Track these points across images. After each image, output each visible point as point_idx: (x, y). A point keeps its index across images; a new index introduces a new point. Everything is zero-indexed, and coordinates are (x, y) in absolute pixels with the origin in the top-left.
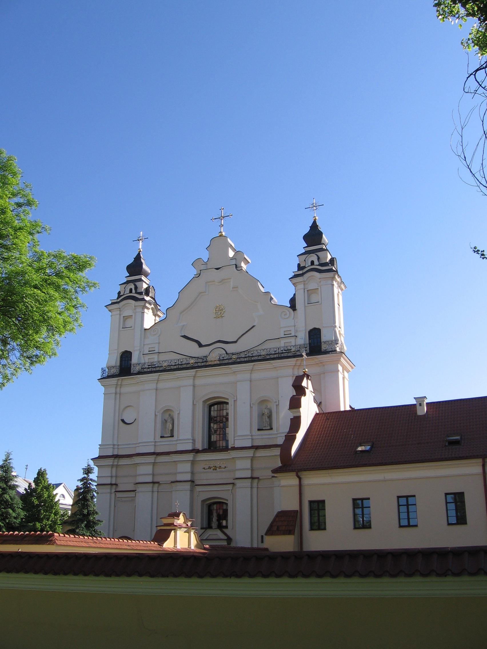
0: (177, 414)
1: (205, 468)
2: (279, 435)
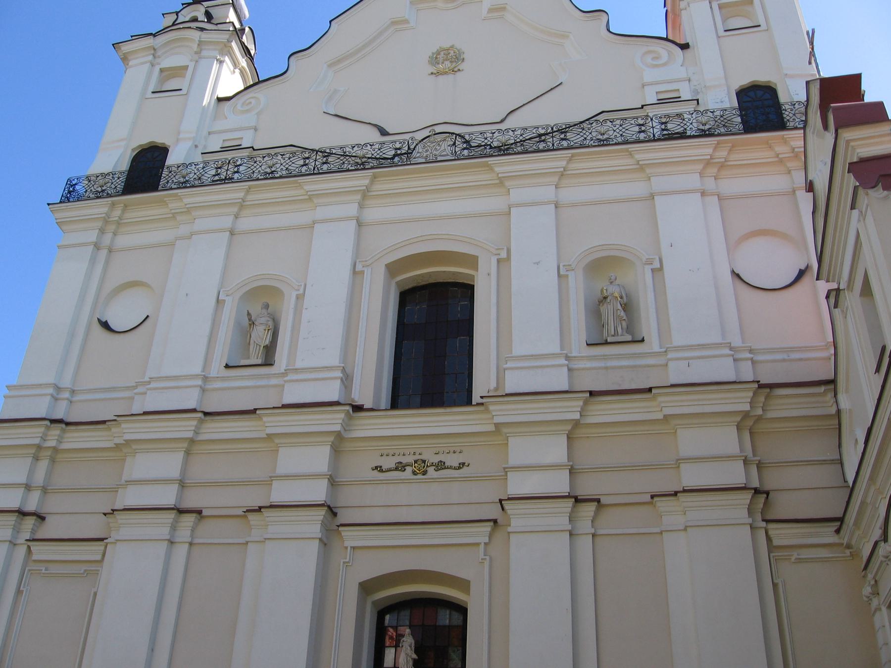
0: (294, 299)
1: (381, 467)
2: (671, 355)
